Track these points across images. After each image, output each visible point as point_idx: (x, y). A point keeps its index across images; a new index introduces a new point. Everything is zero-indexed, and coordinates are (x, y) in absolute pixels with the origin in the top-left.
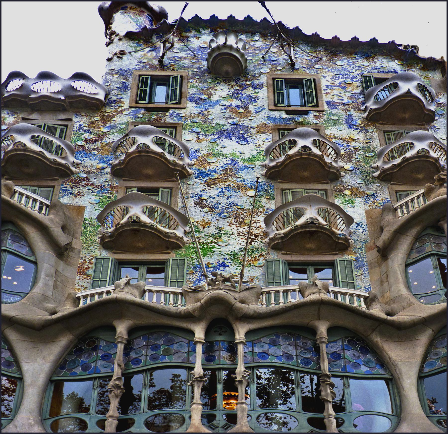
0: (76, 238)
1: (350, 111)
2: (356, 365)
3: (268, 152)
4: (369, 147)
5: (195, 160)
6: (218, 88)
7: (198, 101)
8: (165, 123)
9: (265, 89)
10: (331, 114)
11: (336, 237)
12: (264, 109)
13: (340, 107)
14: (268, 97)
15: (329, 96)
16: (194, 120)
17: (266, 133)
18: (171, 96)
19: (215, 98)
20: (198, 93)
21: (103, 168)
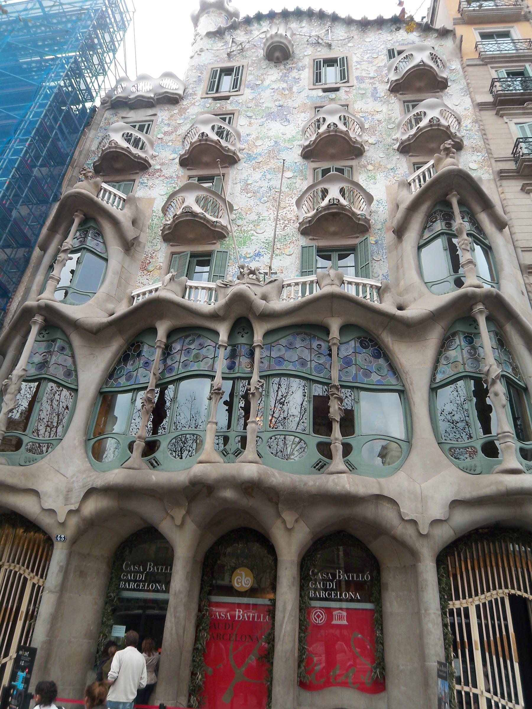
0: (143, 232)
1: (375, 84)
2: (367, 373)
3: (304, 132)
4: (390, 119)
6: (269, 73)
7: (252, 88)
8: (226, 110)
9: (307, 70)
10: (360, 88)
11: (357, 218)
14: (309, 77)
15: (359, 71)
17: (305, 112)
18: (235, 85)
19: (267, 83)
20: (254, 79)
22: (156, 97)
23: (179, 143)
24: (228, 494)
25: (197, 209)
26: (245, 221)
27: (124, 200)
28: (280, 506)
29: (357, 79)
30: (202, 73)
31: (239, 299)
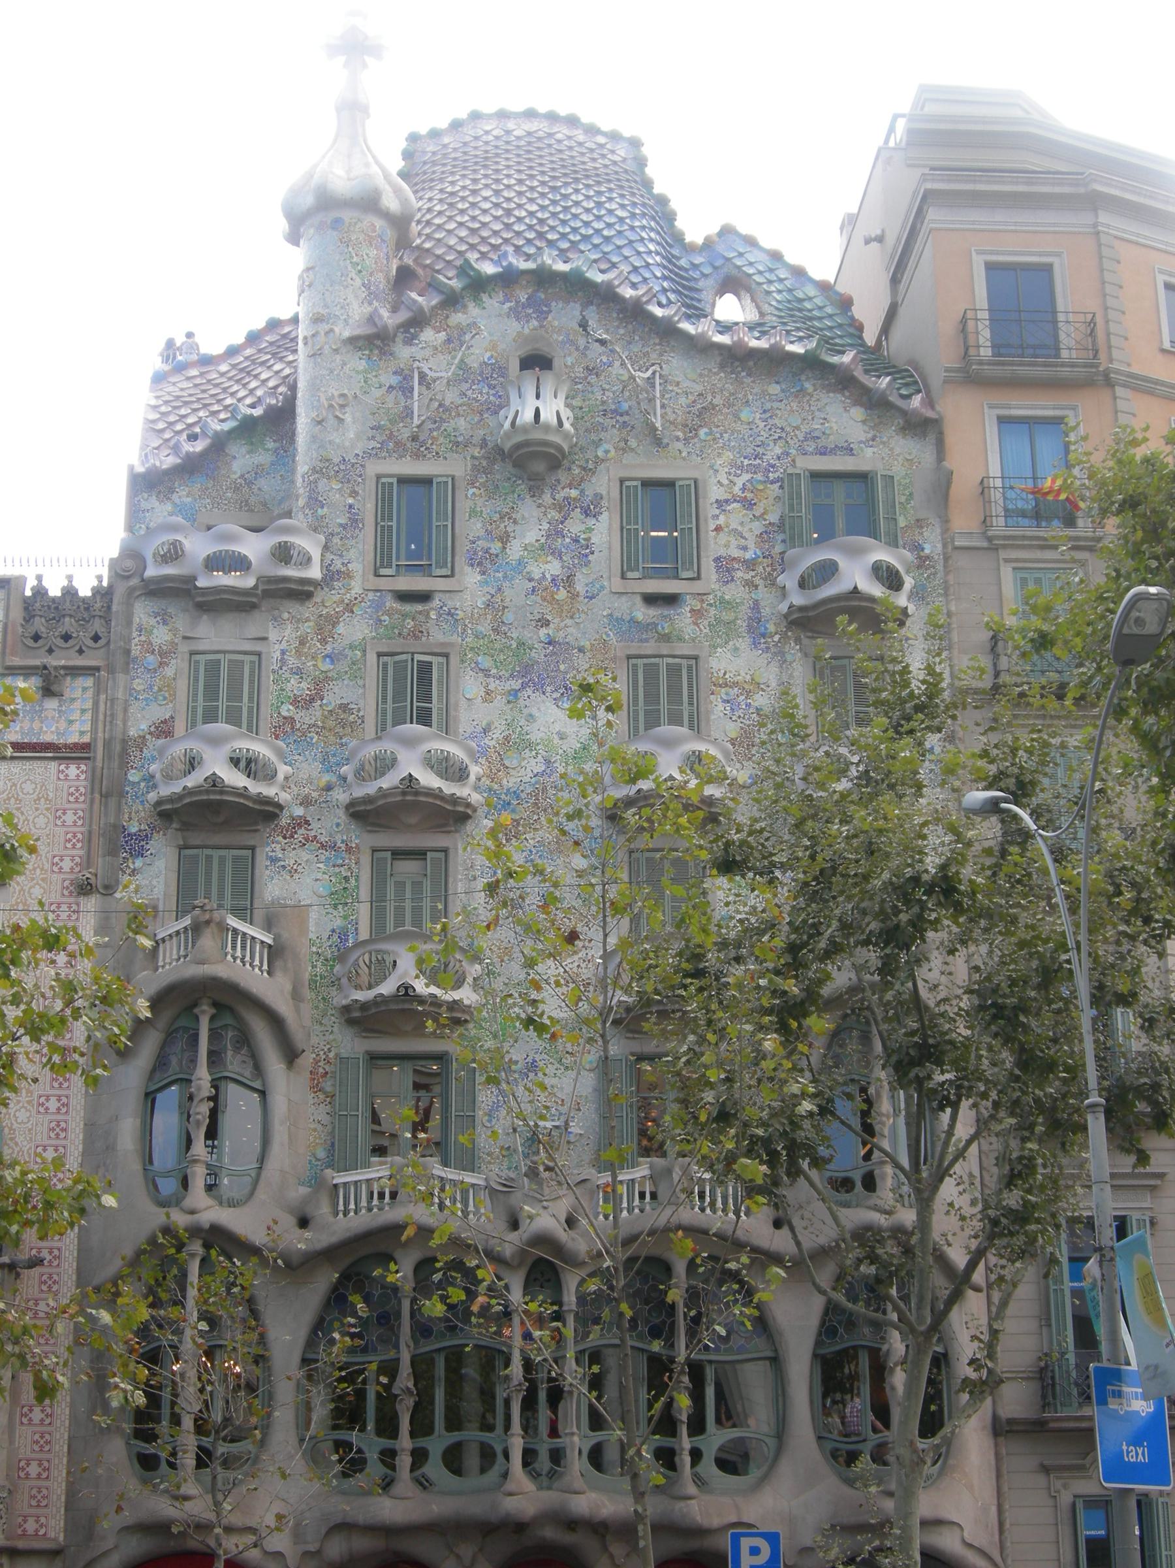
5: (482, 760)
7: (483, 561)
9: (604, 517)
10: (722, 601)
12: (603, 587)
13: (739, 574)
15: (723, 538)
16: (480, 628)
19: (515, 551)
20: (482, 533)
21: (329, 788)
22: (261, 588)
23: (332, 738)
24: (549, 1533)
25: (421, 987)
26: (501, 980)
27: (270, 946)
28: (608, 1537)
29: (718, 568)
30: (354, 494)
31: (543, 1240)
